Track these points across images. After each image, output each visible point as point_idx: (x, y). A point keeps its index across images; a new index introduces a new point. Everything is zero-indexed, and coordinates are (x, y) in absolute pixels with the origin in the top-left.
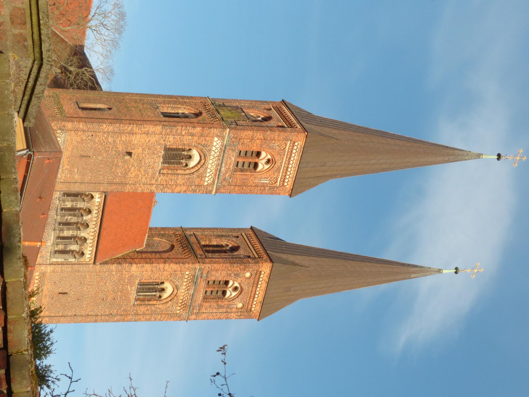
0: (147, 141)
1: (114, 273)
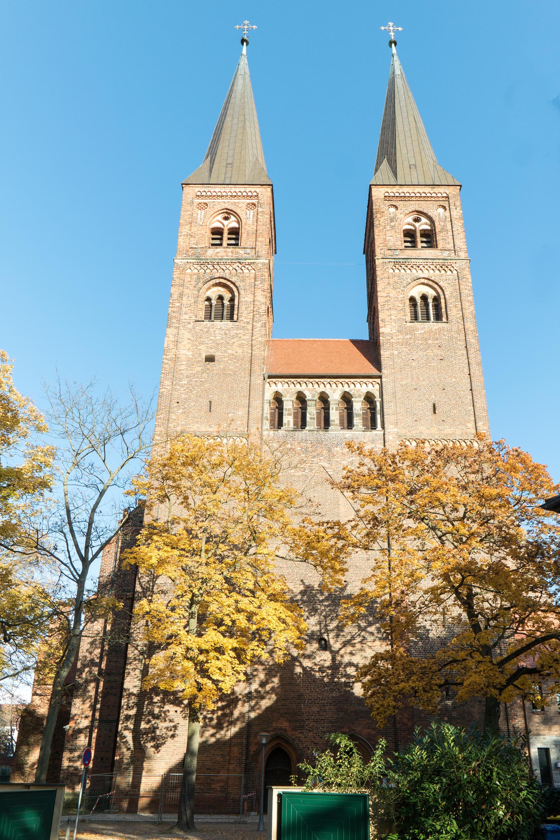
0: (189, 341)
1: (396, 352)
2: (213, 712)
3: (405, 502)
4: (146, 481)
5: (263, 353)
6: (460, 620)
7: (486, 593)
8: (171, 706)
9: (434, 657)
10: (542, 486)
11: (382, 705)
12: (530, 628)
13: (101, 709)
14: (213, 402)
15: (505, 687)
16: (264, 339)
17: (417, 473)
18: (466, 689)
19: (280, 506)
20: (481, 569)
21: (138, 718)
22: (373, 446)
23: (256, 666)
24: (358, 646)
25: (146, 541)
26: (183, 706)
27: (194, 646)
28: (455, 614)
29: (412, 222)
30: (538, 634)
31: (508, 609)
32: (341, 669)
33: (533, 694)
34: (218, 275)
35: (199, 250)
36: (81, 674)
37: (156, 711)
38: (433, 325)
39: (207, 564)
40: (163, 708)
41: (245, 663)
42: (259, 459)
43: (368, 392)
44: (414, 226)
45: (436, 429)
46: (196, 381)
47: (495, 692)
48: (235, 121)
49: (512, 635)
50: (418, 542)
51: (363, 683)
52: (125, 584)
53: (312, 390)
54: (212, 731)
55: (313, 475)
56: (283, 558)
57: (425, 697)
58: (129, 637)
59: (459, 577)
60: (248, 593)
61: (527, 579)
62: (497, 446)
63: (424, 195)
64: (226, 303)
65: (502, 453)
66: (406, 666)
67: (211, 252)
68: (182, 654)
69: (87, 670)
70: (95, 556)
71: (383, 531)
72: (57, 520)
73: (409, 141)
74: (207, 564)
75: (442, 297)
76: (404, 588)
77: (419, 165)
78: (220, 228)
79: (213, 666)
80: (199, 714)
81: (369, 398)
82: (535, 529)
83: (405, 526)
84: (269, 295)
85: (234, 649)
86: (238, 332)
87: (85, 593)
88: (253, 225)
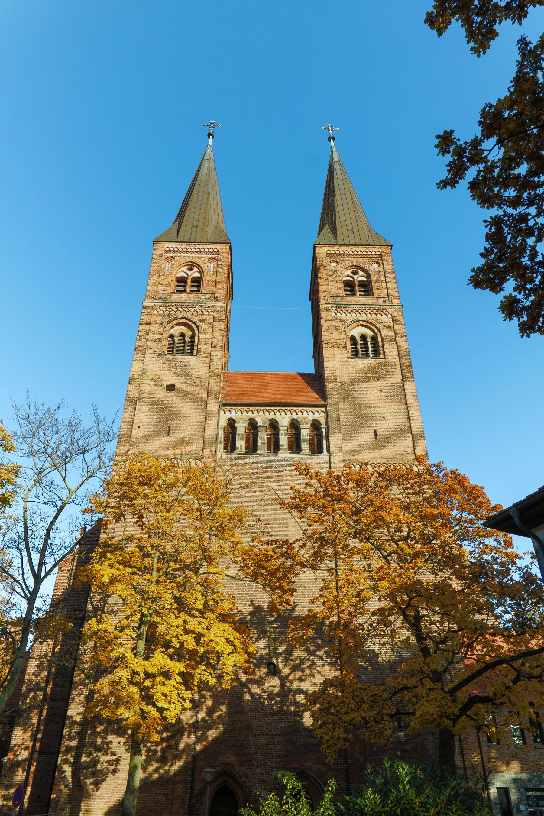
1: (339, 384)
2: (157, 744)
3: (351, 522)
4: (104, 499)
5: (219, 384)
6: (409, 644)
7: (434, 615)
8: (115, 736)
9: (384, 684)
10: (481, 507)
11: (332, 737)
12: (479, 653)
13: (42, 739)
14: (171, 427)
15: (458, 717)
16: (220, 371)
17: (361, 493)
18: (419, 720)
19: (231, 526)
20: (427, 590)
21: (79, 751)
22: (320, 469)
23: (204, 692)
24: (308, 671)
25: (100, 559)
26: (127, 736)
27: (140, 669)
28: (403, 637)
29: (350, 274)
30: (488, 658)
31: (456, 632)
32: (290, 697)
33: (487, 726)
34: (181, 316)
35: (165, 295)
36: (26, 699)
37: (99, 741)
38: (371, 361)
39: (158, 582)
40: (106, 738)
41: (192, 690)
42: (212, 479)
43: (314, 420)
44: (353, 278)
45: (377, 454)
46: (157, 408)
47: (448, 723)
48: (201, 194)
49: (462, 660)
50: (364, 563)
51: (312, 712)
52: (76, 602)
53: (263, 417)
54: (155, 765)
55: (263, 496)
56: (232, 577)
57: (376, 728)
58: (76, 659)
59: (405, 597)
60: (197, 614)
61: (473, 601)
62: (435, 468)
63: (360, 253)
64: (187, 339)
65: (441, 475)
66: (356, 693)
67: (175, 297)
68: (128, 679)
69: (31, 694)
70: (48, 574)
71: (330, 551)
72: (15, 536)
73: (346, 211)
74: (158, 582)
75: (379, 336)
76: (351, 609)
77: (355, 229)
78: (185, 277)
79: (159, 691)
80: (141, 747)
81: (315, 425)
82: (477, 550)
83: (352, 546)
84: (225, 334)
85: (181, 674)
86: (197, 365)
87: (35, 611)
88: (213, 275)
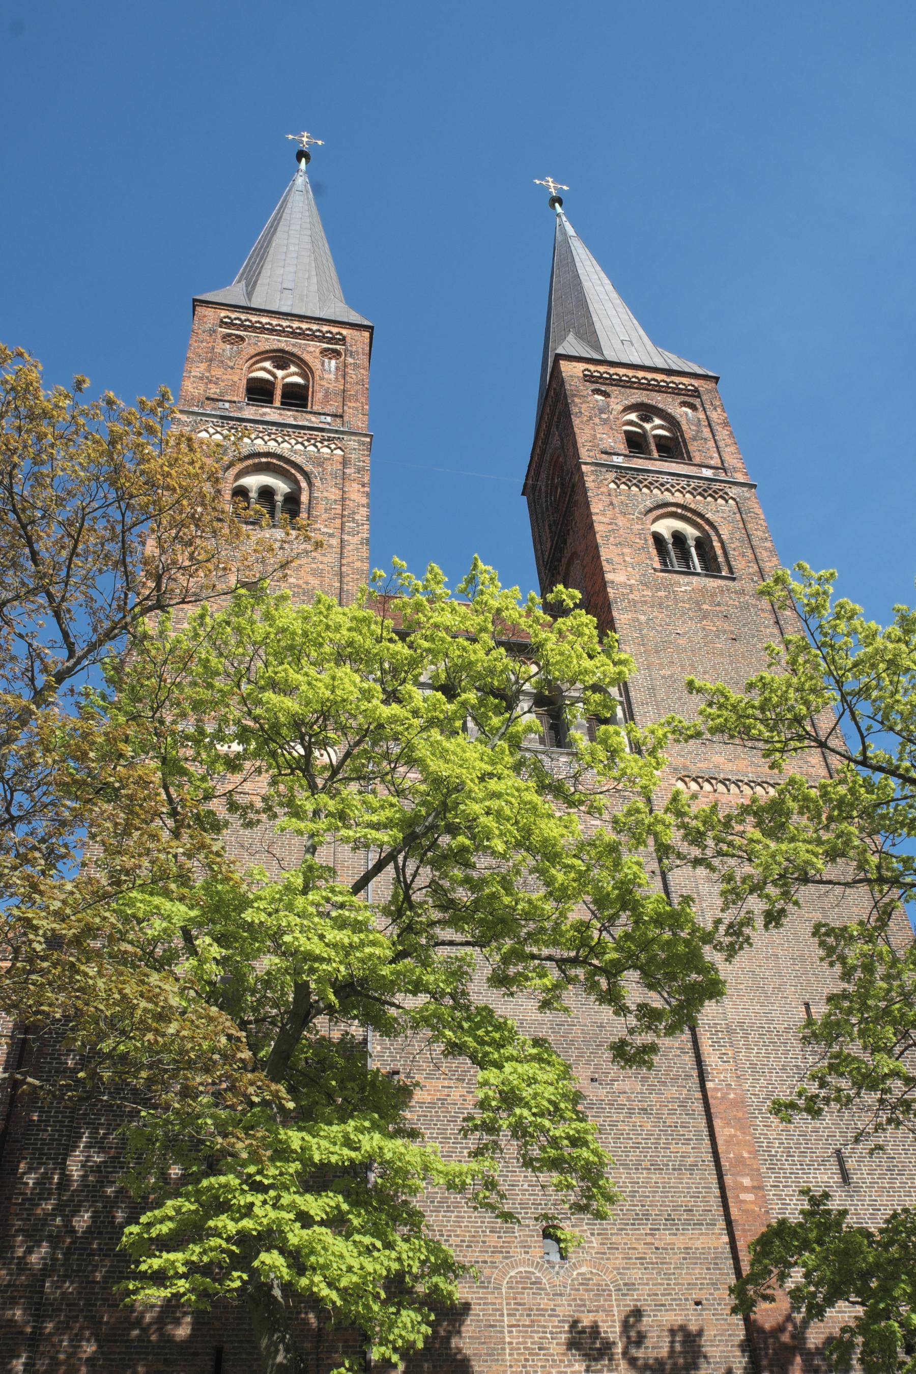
44: (641, 427)
78: (267, 381)
